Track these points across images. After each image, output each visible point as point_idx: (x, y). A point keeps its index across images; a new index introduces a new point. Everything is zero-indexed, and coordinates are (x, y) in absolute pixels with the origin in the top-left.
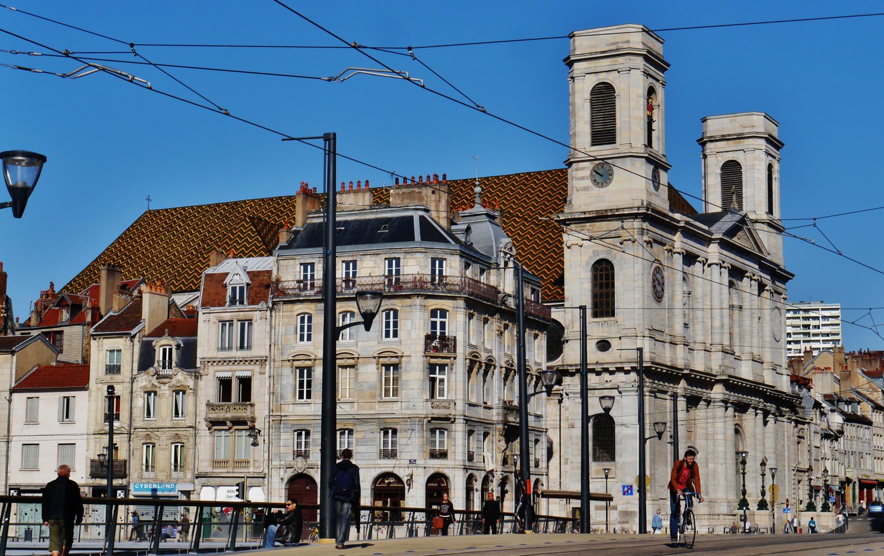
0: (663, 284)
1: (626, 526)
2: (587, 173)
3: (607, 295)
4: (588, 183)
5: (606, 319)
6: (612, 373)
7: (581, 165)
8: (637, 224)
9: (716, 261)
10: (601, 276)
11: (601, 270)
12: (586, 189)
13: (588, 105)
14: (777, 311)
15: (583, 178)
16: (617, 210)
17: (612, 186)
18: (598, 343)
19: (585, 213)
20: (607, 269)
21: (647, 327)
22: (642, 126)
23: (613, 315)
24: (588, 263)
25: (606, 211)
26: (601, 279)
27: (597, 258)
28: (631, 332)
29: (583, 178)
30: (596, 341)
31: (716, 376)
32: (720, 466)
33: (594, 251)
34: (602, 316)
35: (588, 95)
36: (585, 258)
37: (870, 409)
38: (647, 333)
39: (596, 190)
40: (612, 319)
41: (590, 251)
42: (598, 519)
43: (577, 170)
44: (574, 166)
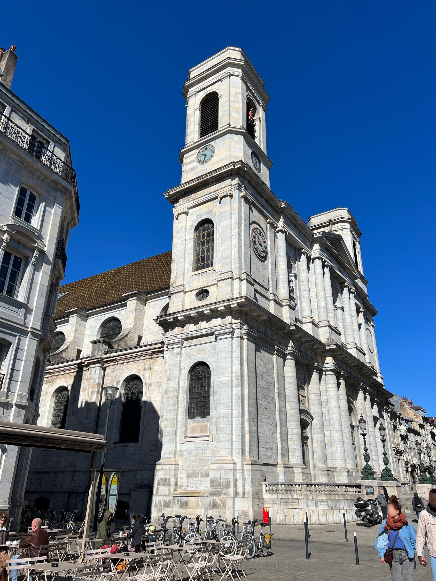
0: (266, 248)
1: (217, 499)
2: (195, 157)
3: (208, 250)
4: (195, 164)
5: (205, 270)
6: (208, 318)
7: (190, 154)
8: (236, 181)
9: (318, 255)
10: (203, 235)
11: (204, 230)
12: (193, 169)
13: (198, 114)
14: (368, 330)
15: (191, 162)
16: (215, 171)
17: (214, 160)
18: (198, 295)
19: (188, 182)
20: (208, 228)
21: (244, 271)
22: (241, 114)
23: (212, 265)
24: (191, 226)
25: (206, 175)
26: (203, 237)
27: (200, 220)
28: (228, 275)
29: (191, 162)
30: (196, 292)
31: (325, 346)
32: (336, 434)
33: (197, 215)
34: (203, 268)
35: (198, 105)
36: (189, 223)
37: (418, 426)
38: (244, 276)
39: (201, 167)
40: (210, 268)
41: (194, 217)
42: (189, 489)
43: (186, 158)
44: (185, 156)
